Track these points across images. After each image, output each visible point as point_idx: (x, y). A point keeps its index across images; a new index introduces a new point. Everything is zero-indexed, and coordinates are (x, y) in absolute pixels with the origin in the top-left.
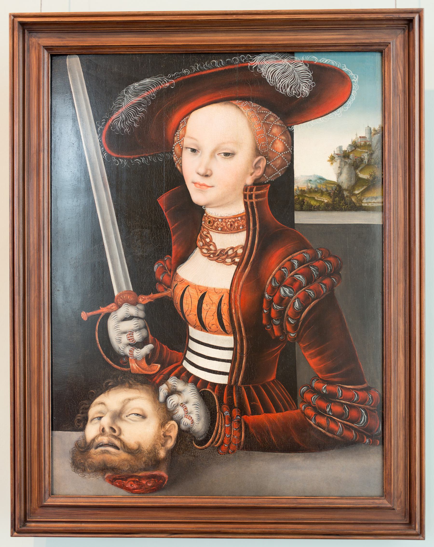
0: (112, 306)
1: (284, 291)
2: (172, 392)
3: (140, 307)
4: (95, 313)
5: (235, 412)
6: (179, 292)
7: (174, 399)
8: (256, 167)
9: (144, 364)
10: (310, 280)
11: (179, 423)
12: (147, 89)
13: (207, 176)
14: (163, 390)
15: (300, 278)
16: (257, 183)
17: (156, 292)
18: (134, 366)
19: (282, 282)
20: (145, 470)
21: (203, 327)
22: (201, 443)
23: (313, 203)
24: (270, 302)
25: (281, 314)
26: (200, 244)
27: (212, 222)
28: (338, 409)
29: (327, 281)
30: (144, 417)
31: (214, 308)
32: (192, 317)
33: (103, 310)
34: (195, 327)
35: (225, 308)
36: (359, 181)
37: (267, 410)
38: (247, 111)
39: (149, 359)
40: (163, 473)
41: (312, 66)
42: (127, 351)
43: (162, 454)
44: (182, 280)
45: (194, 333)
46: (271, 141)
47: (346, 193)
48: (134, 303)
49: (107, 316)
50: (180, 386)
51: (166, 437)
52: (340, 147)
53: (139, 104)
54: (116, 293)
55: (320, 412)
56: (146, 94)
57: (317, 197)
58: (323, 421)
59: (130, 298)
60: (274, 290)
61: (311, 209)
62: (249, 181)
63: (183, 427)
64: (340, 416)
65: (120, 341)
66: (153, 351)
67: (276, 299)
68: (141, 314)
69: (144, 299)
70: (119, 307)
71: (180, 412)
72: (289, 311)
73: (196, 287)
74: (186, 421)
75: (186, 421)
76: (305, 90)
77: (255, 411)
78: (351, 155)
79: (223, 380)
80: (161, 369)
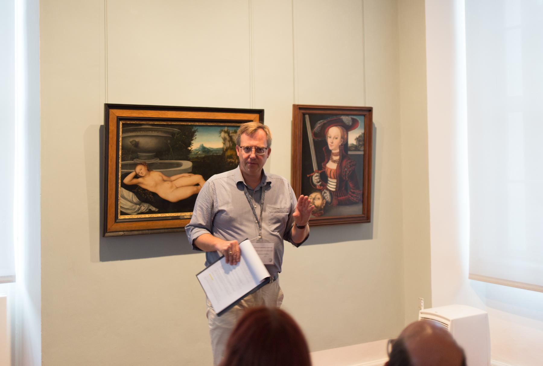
0: (314, 173)
1: (346, 169)
2: (325, 193)
3: (319, 173)
4: (310, 175)
5: (336, 197)
6: (326, 169)
7: (325, 195)
8: (341, 141)
9: (320, 187)
10: (351, 167)
11: (326, 200)
12: (321, 123)
13: (332, 143)
14: (323, 192)
15: (349, 166)
16: (342, 145)
17: (322, 170)
18: (318, 187)
19: (345, 167)
20: (319, 211)
21: (331, 178)
22: (330, 204)
23: (352, 149)
24: (343, 172)
25: (345, 174)
26: (331, 158)
27: (333, 154)
28: (355, 195)
29: (354, 167)
30: (319, 199)
31: (333, 173)
32: (329, 175)
33: (312, 174)
34: (329, 178)
35: (335, 173)
36: (360, 145)
37: (342, 196)
38: (340, 128)
39: (321, 185)
40: (322, 212)
41: (353, 119)
42: (316, 184)
43: (322, 207)
44: (327, 167)
45: (329, 179)
46: (344, 136)
47: (358, 147)
48: (318, 173)
49: (312, 176)
50: (326, 191)
51: (323, 203)
52: (357, 137)
53: (320, 126)
54: (314, 170)
55: (351, 196)
56: (321, 124)
57: (352, 148)
58: (352, 198)
59: (317, 171)
60: (344, 169)
61: (351, 151)
62: (340, 144)
63: (327, 201)
64: (356, 197)
65: (315, 181)
66: (321, 184)
67: (344, 171)
68: (319, 175)
69: (320, 172)
70: (315, 173)
71: (326, 197)
72: (347, 174)
73: (330, 169)
74: (327, 199)
75: (327, 199)
76: (351, 124)
77: (340, 197)
78: (359, 139)
79: (334, 190)
80: (323, 187)
